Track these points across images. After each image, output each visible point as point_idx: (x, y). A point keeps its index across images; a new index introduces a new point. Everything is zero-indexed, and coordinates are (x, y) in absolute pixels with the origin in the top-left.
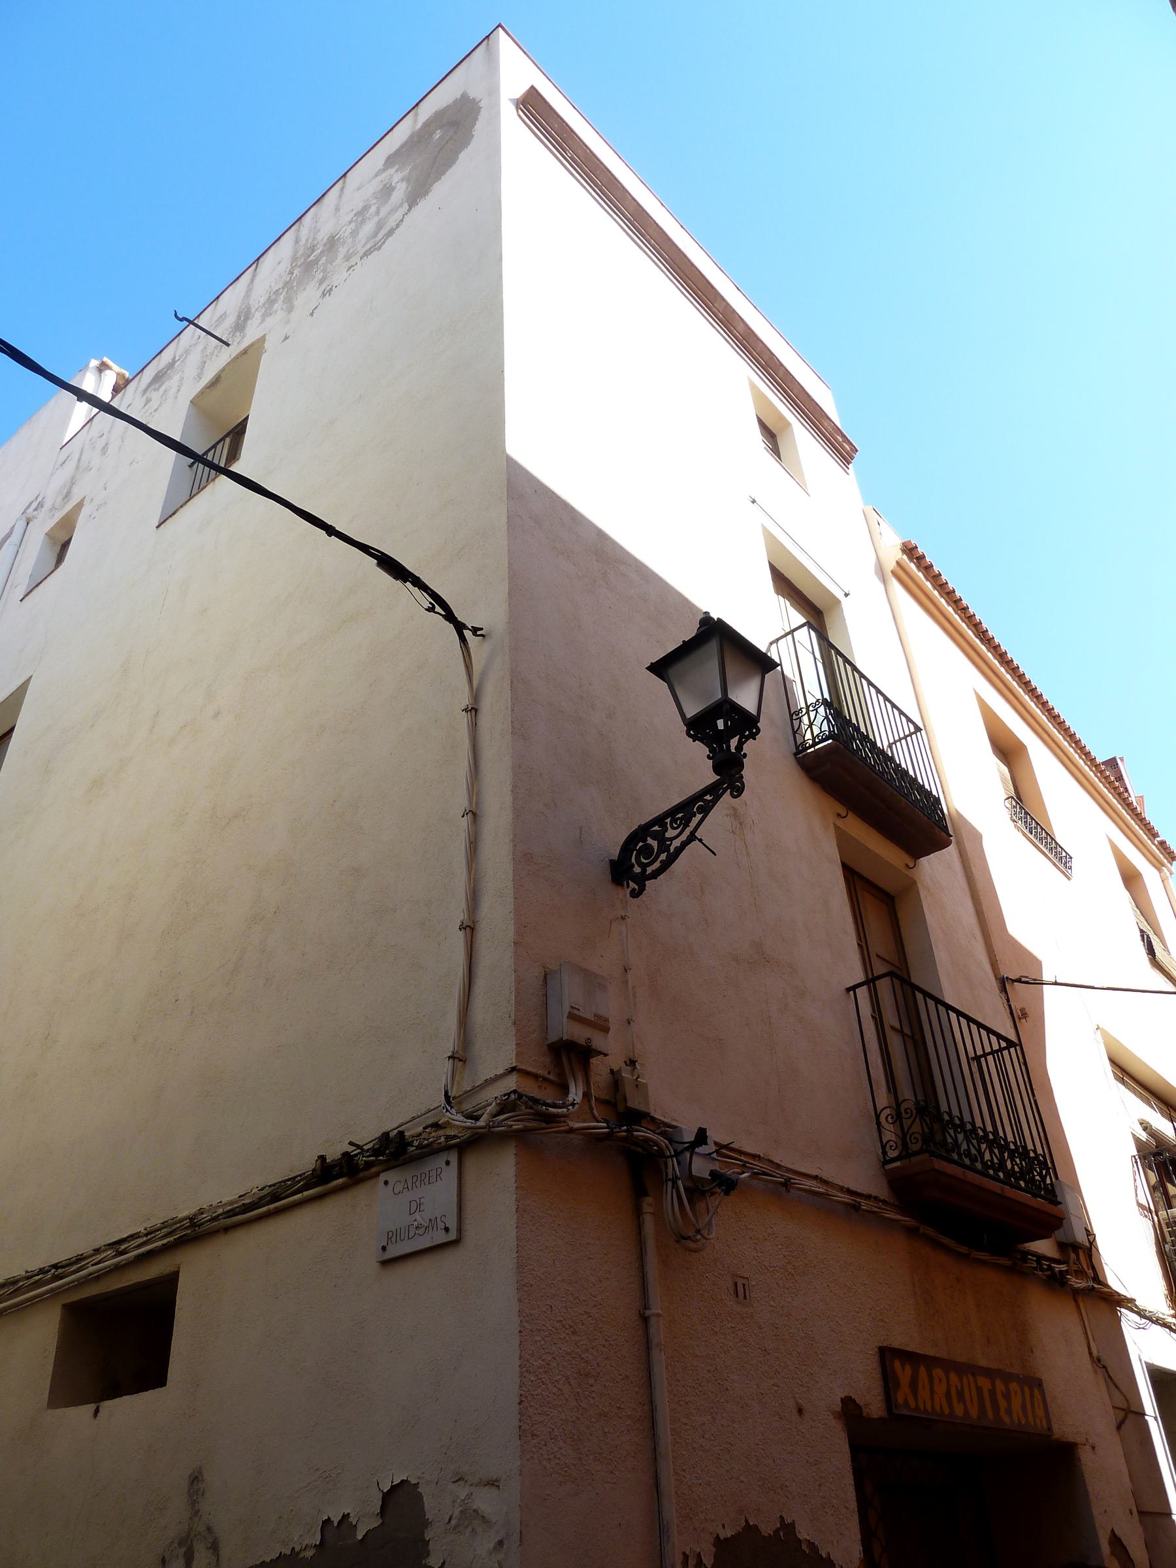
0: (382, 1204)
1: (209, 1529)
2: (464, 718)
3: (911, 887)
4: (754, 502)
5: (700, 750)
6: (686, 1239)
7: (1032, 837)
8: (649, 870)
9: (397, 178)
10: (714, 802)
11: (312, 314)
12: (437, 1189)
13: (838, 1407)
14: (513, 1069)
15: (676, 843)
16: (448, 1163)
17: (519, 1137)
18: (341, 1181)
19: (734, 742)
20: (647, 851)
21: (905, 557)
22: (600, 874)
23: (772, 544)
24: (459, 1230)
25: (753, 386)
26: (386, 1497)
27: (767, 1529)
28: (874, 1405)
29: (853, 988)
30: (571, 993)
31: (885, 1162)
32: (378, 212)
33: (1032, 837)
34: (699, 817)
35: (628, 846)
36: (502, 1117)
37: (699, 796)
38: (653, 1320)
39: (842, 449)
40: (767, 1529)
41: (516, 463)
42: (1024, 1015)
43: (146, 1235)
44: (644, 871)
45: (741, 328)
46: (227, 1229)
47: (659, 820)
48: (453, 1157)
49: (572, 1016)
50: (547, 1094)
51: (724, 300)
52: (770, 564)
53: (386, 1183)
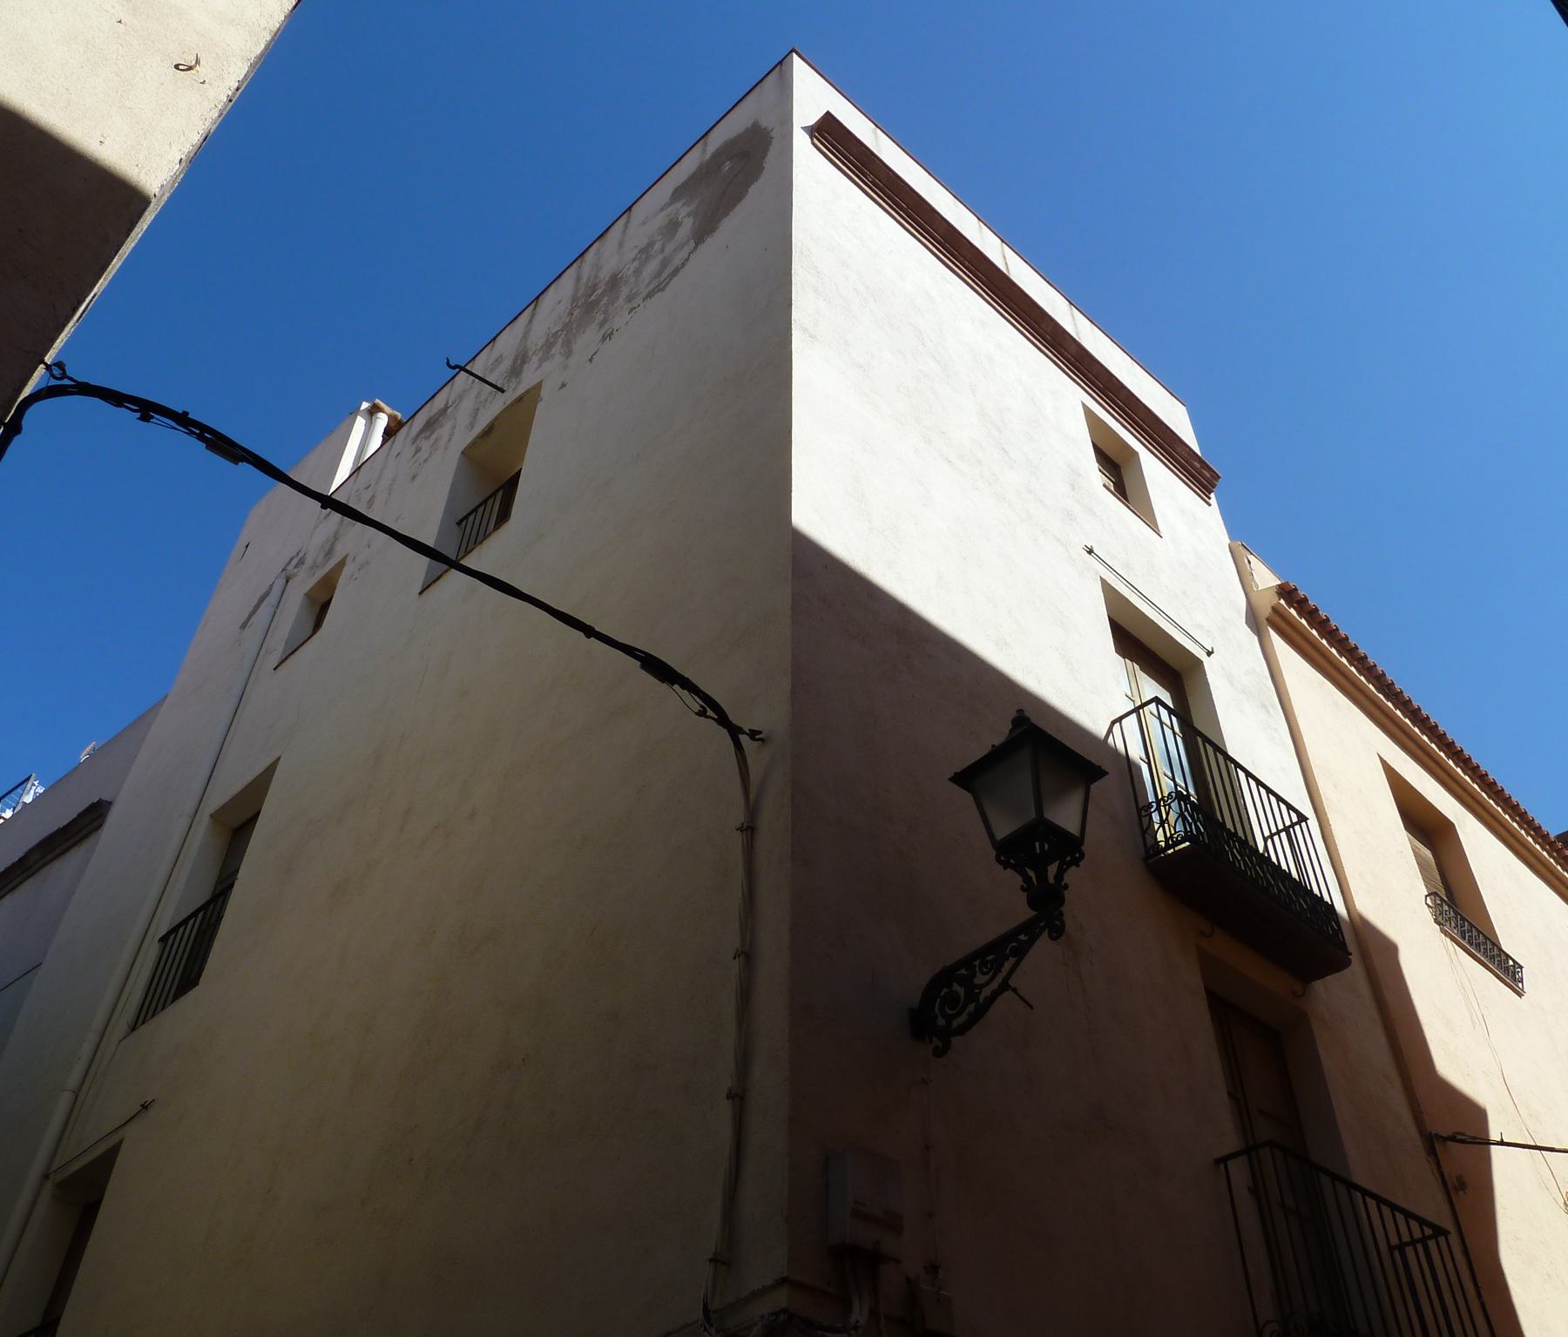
2: (737, 840)
5: (1013, 879)
8: (955, 1023)
15: (986, 992)
19: (1052, 869)
29: (1223, 1160)
34: (1012, 960)
37: (1010, 936)
42: (1462, 1185)
47: (966, 962)
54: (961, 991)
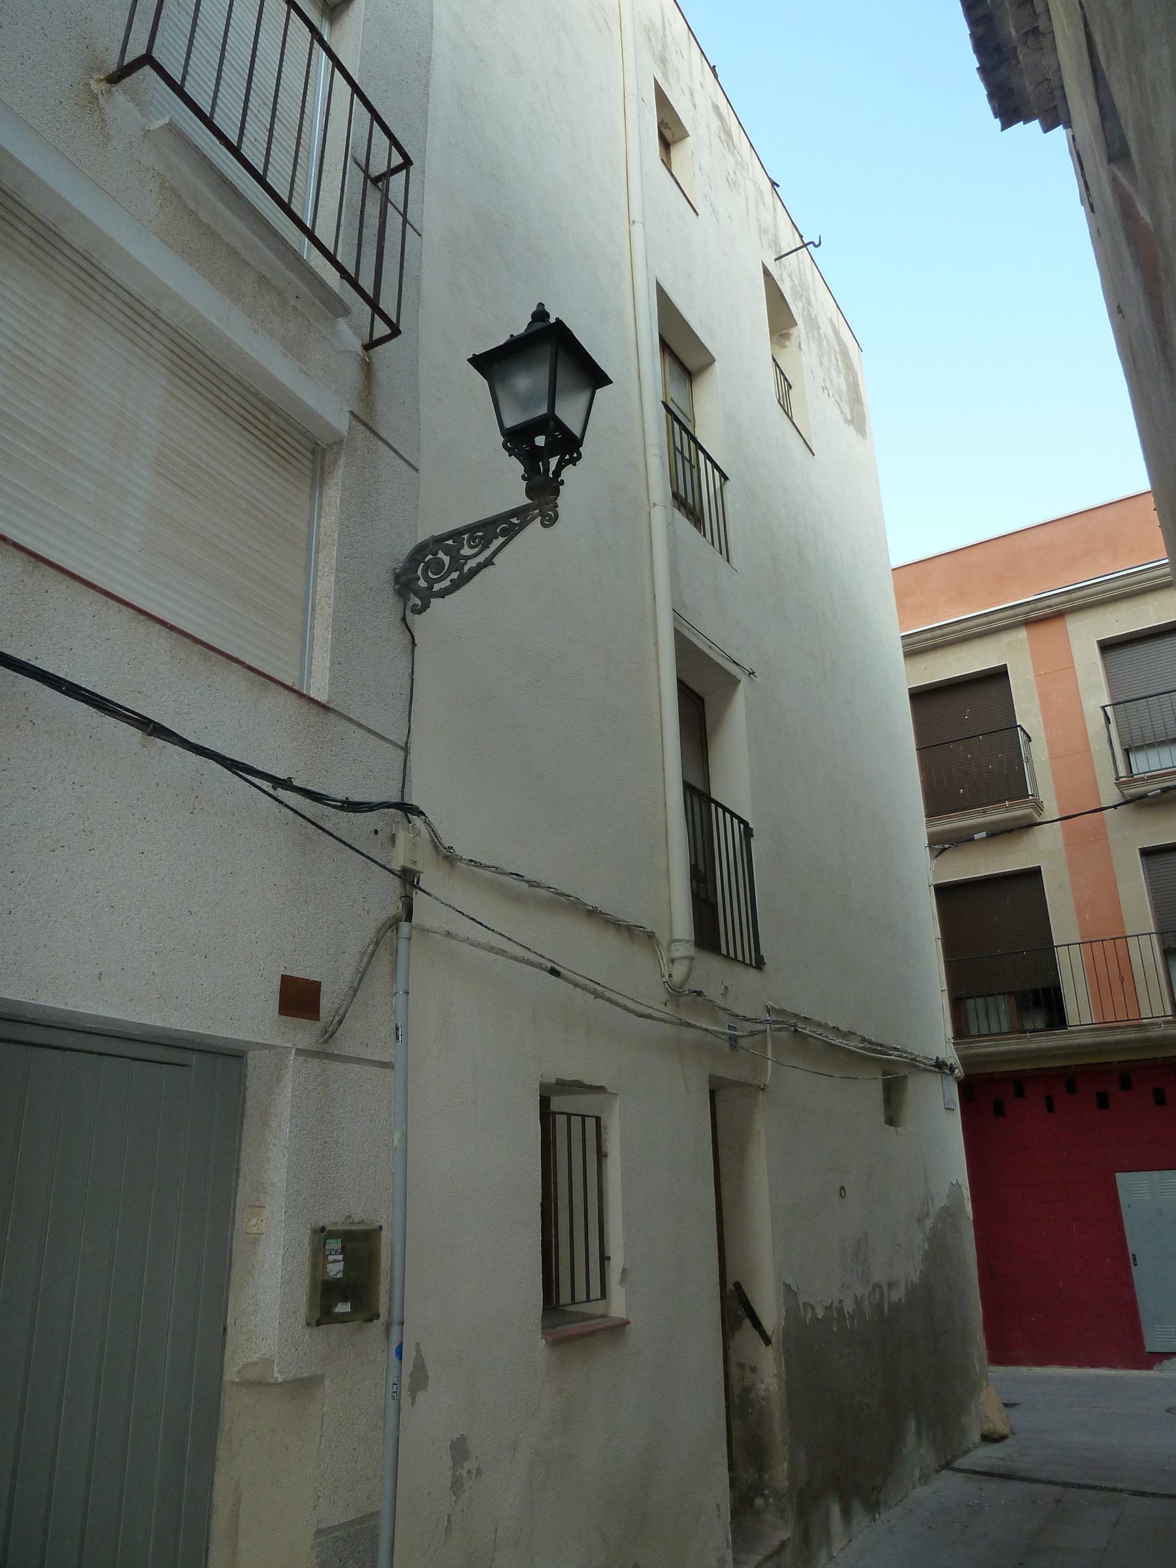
8: (437, 587)
10: (522, 526)
15: (472, 563)
19: (554, 462)
34: (501, 540)
47: (456, 535)
54: (447, 560)
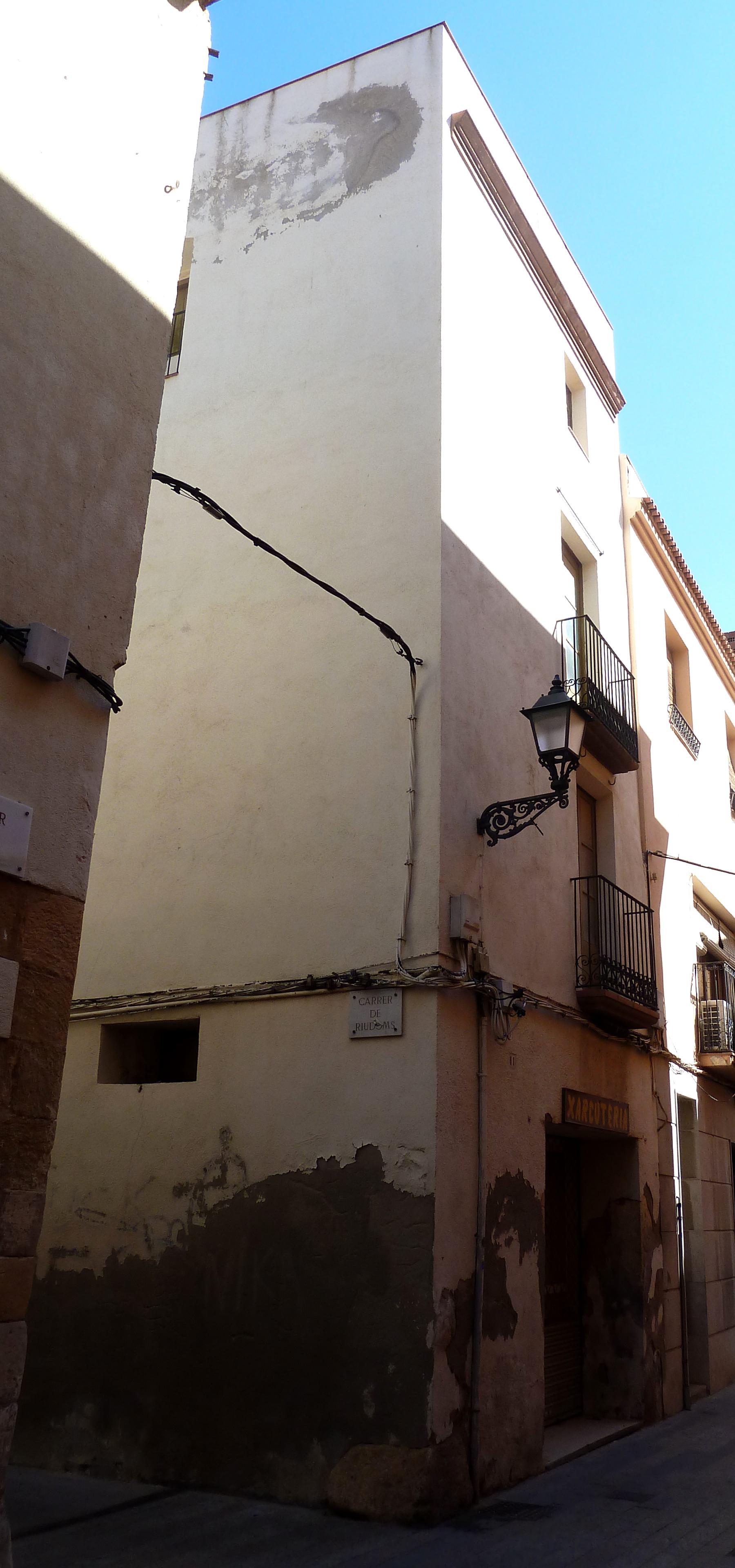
0: (347, 1008)
1: (237, 1156)
2: (409, 724)
3: (608, 796)
4: (559, 491)
5: (546, 773)
6: (501, 1038)
7: (679, 733)
8: (501, 833)
9: (334, 140)
10: (550, 804)
11: (246, 250)
12: (390, 1008)
13: (543, 1118)
14: (438, 953)
16: (396, 995)
17: (440, 990)
18: (322, 990)
20: (501, 820)
21: (643, 510)
22: (472, 826)
23: (567, 527)
24: (402, 1031)
25: (567, 359)
26: (359, 1151)
27: (513, 1175)
28: (557, 1119)
29: (575, 879)
30: (467, 913)
31: (577, 987)
32: (314, 172)
33: (679, 733)
35: (487, 813)
36: (432, 979)
37: (538, 798)
38: (483, 1079)
39: (614, 401)
40: (513, 1175)
41: (447, 527)
42: (655, 878)
43: (170, 994)
44: (498, 832)
45: (567, 307)
46: (236, 1002)
47: (512, 803)
48: (400, 993)
49: (466, 926)
50: (448, 966)
51: (561, 284)
52: (563, 540)
53: (354, 997)
54: (506, 817)
